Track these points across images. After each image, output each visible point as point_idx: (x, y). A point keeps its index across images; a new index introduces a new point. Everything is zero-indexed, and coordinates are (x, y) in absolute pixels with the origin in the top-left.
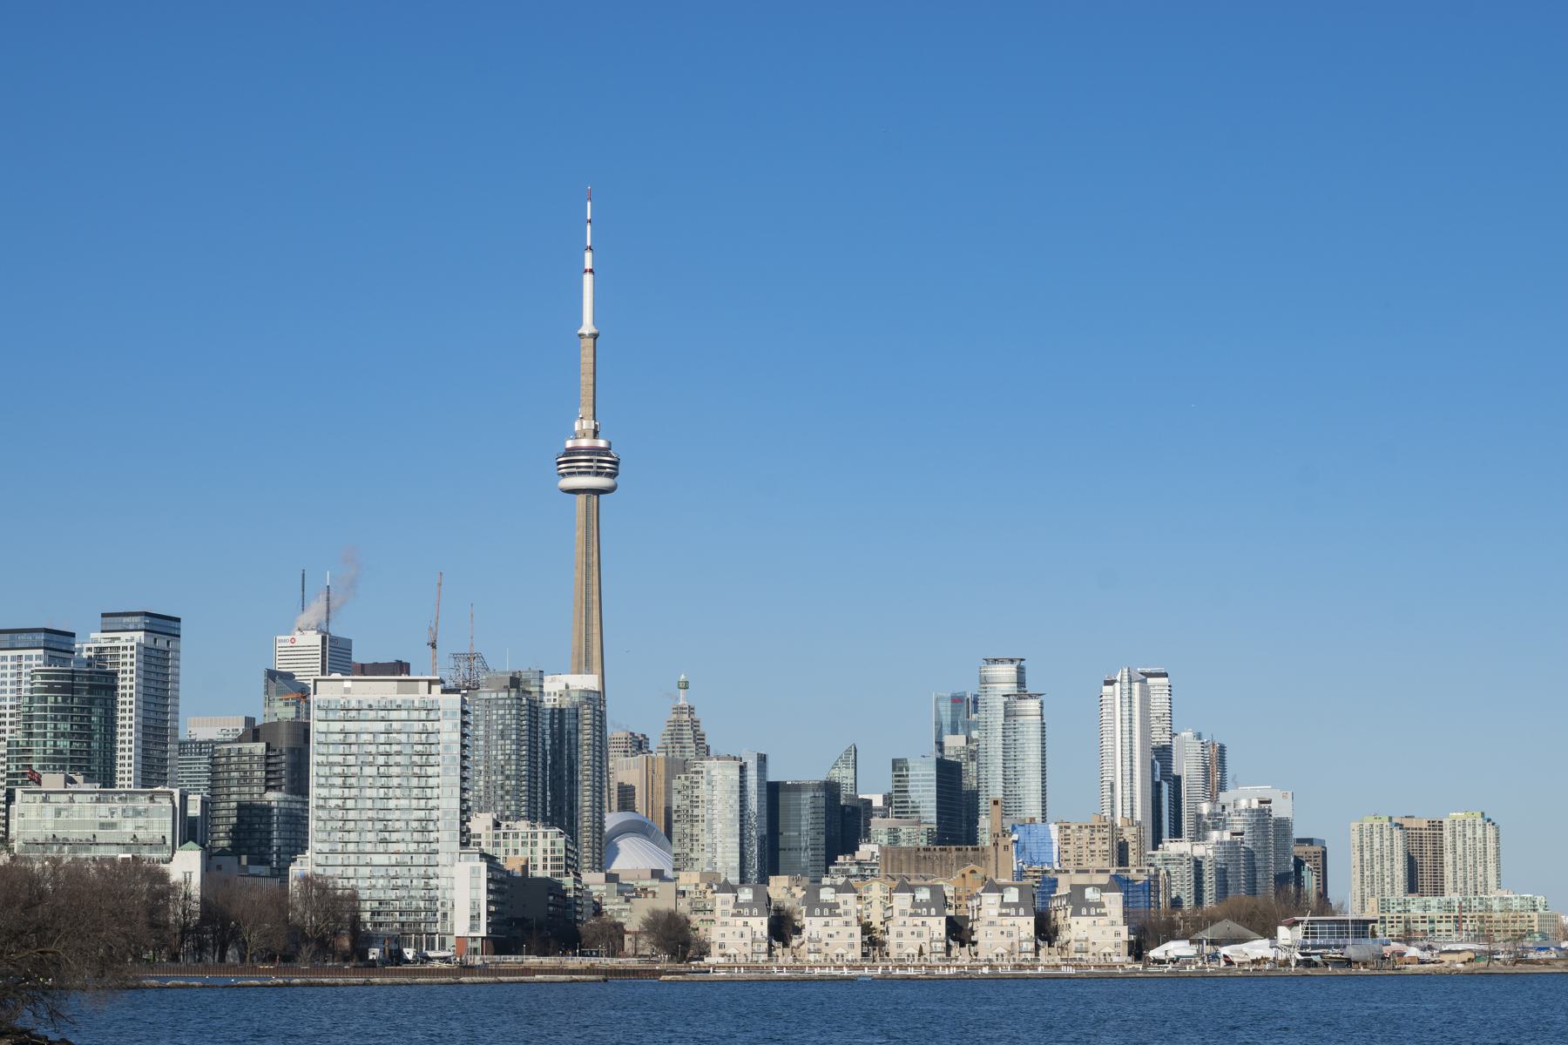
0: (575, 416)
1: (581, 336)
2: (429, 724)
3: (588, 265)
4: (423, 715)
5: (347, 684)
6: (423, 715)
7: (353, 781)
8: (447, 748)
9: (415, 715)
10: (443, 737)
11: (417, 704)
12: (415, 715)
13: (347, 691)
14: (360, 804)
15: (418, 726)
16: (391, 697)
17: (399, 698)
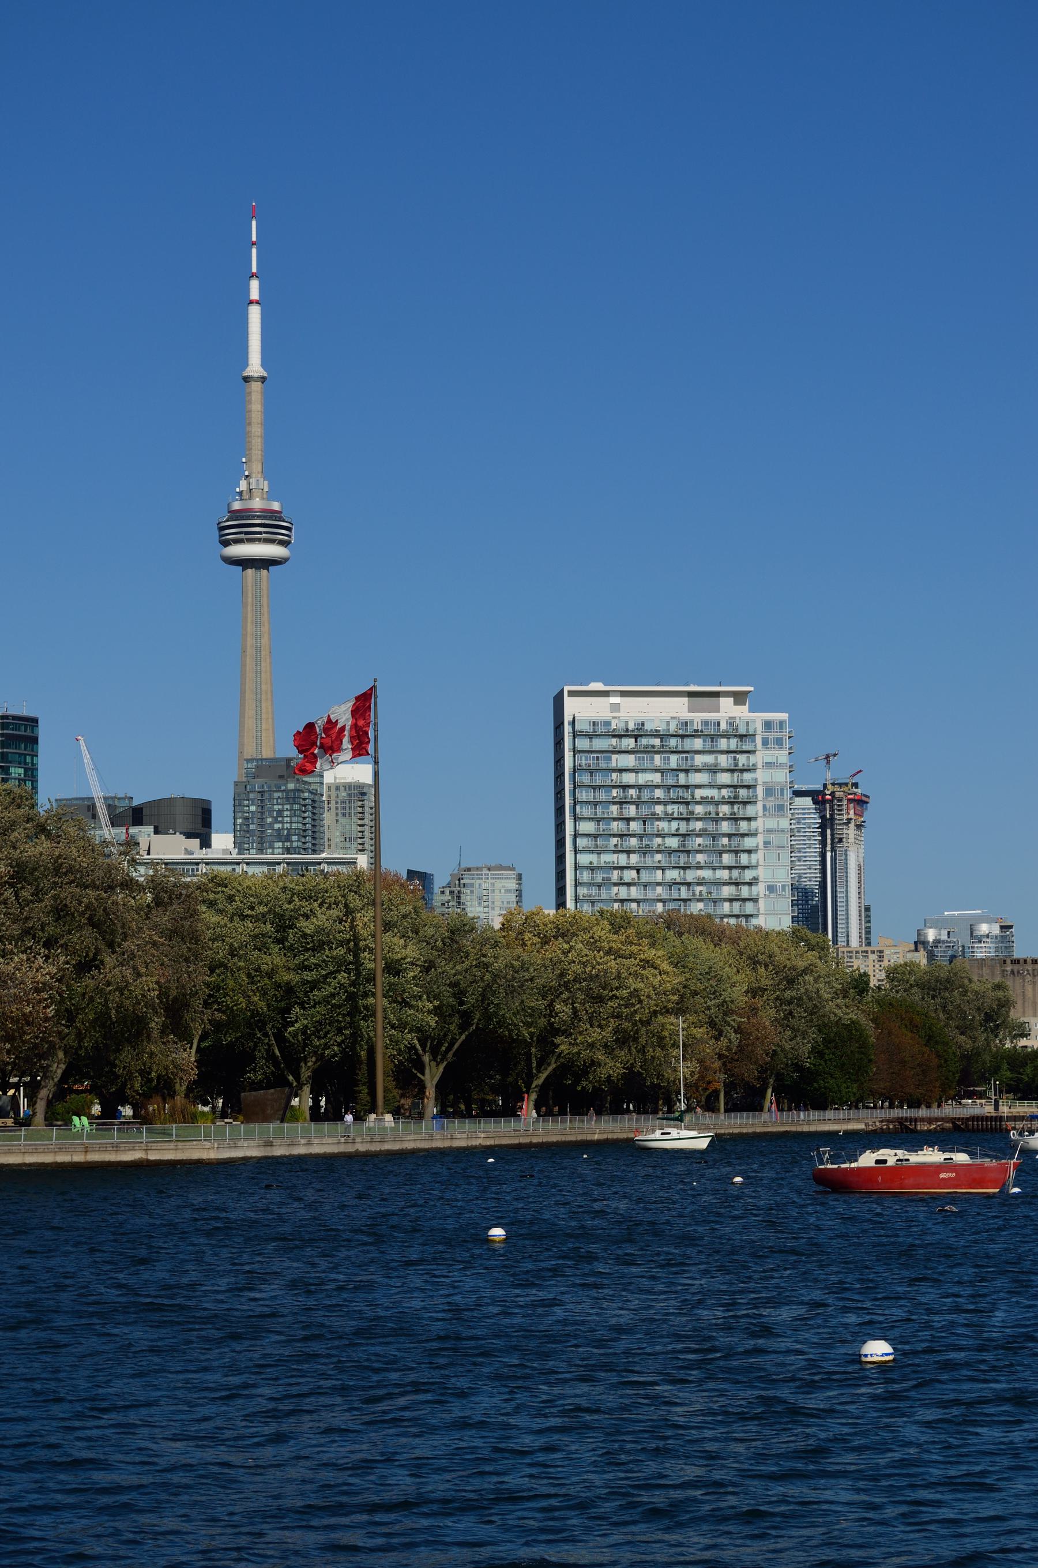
0: (239, 473)
1: (247, 379)
2: (742, 759)
3: (255, 295)
4: (733, 744)
5: (615, 700)
6: (733, 744)
7: (634, 842)
8: (769, 792)
9: (723, 744)
10: (761, 776)
11: (723, 726)
12: (723, 744)
13: (615, 708)
14: (645, 876)
15: (724, 761)
16: (685, 715)
17: (698, 718)
